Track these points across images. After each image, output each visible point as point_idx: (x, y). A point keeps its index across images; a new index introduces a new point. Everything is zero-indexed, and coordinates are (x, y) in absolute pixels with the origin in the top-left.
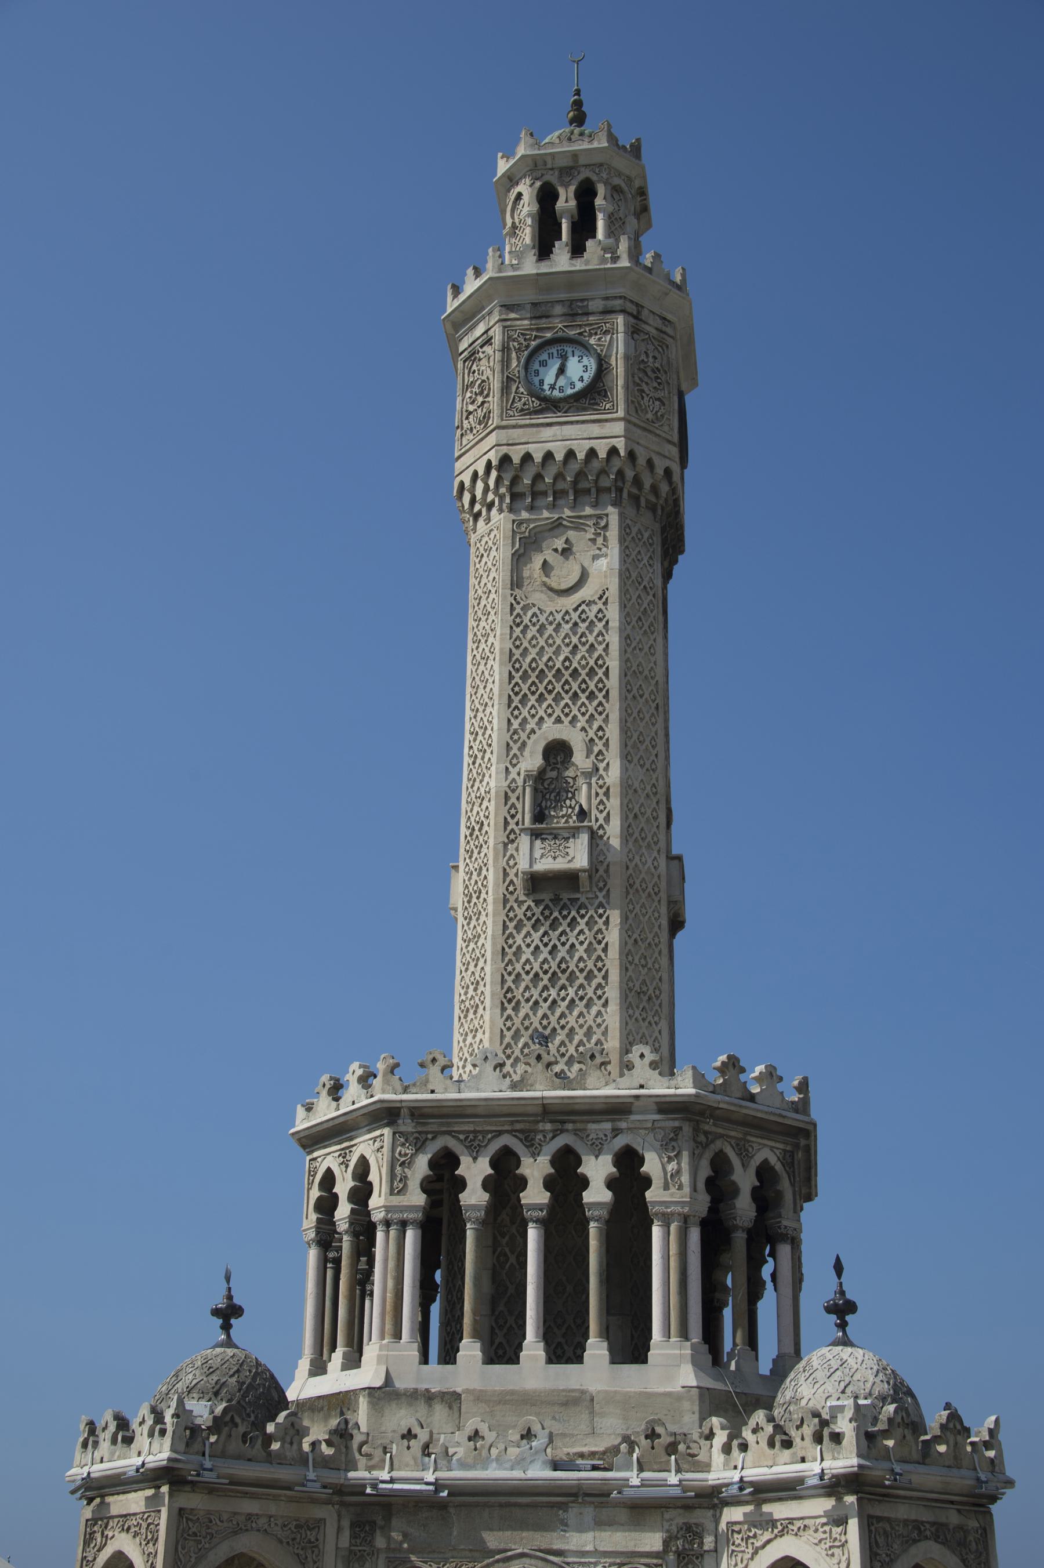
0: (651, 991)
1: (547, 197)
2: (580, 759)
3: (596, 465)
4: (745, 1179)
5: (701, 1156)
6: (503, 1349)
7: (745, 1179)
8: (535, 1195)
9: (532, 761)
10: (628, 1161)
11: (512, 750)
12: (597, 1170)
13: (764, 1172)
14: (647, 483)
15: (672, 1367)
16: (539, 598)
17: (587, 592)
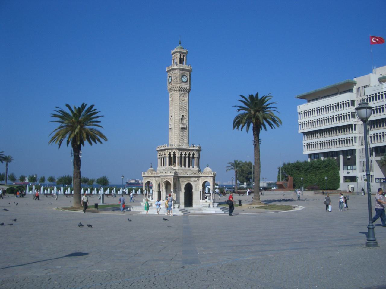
1: (180, 56)
6: (185, 166)
8: (187, 156)
9: (181, 117)
10: (193, 153)
11: (180, 115)
12: (192, 154)
15: (196, 168)
16: (181, 101)
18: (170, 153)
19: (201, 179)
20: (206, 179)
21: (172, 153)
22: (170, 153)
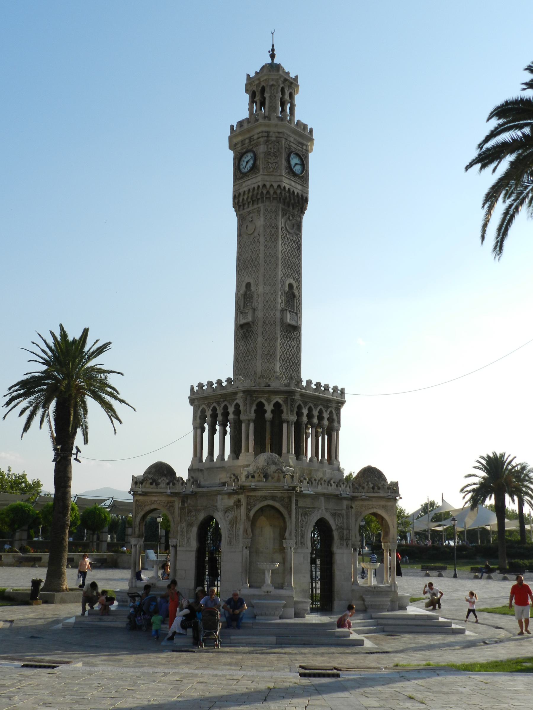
0: (271, 353)
2: (253, 288)
3: (256, 192)
4: (269, 408)
5: (253, 403)
7: (269, 408)
10: (237, 406)
13: (277, 405)
14: (272, 192)
17: (256, 234)
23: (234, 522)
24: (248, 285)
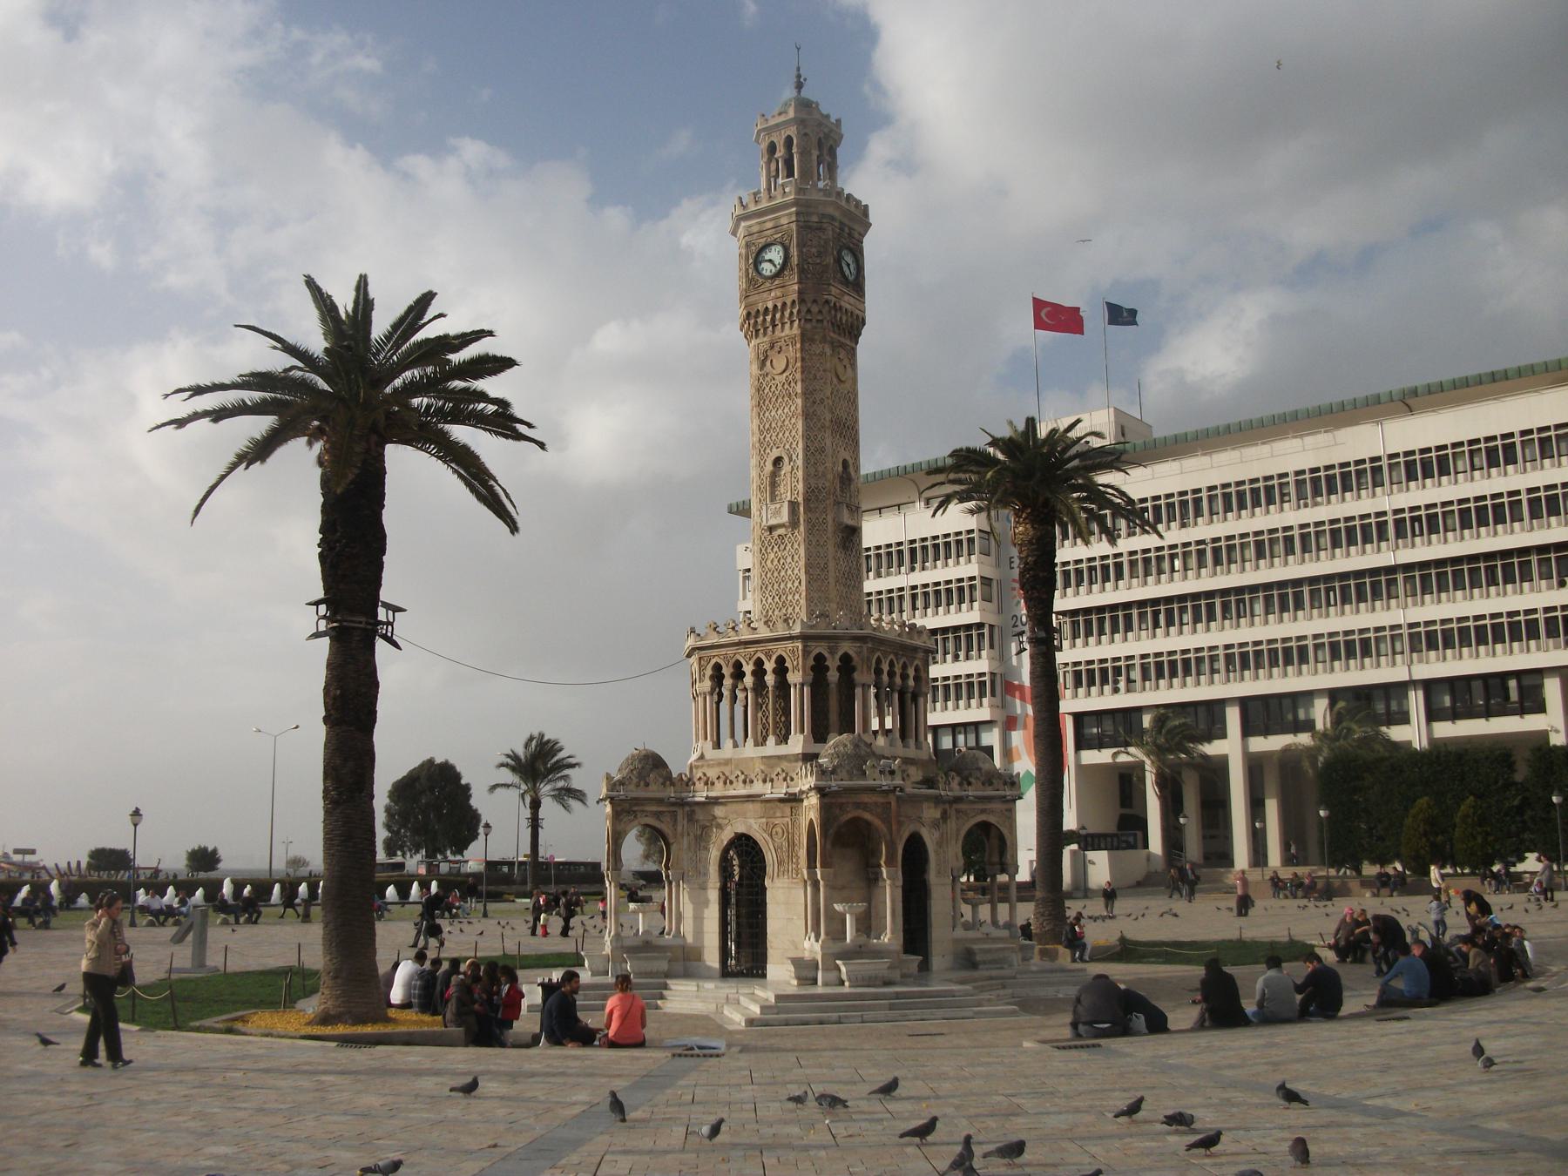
18: (820, 658)
19: (958, 811)
20: (983, 811)
21: (833, 663)
22: (820, 658)
23: (940, 844)
24: (845, 463)
